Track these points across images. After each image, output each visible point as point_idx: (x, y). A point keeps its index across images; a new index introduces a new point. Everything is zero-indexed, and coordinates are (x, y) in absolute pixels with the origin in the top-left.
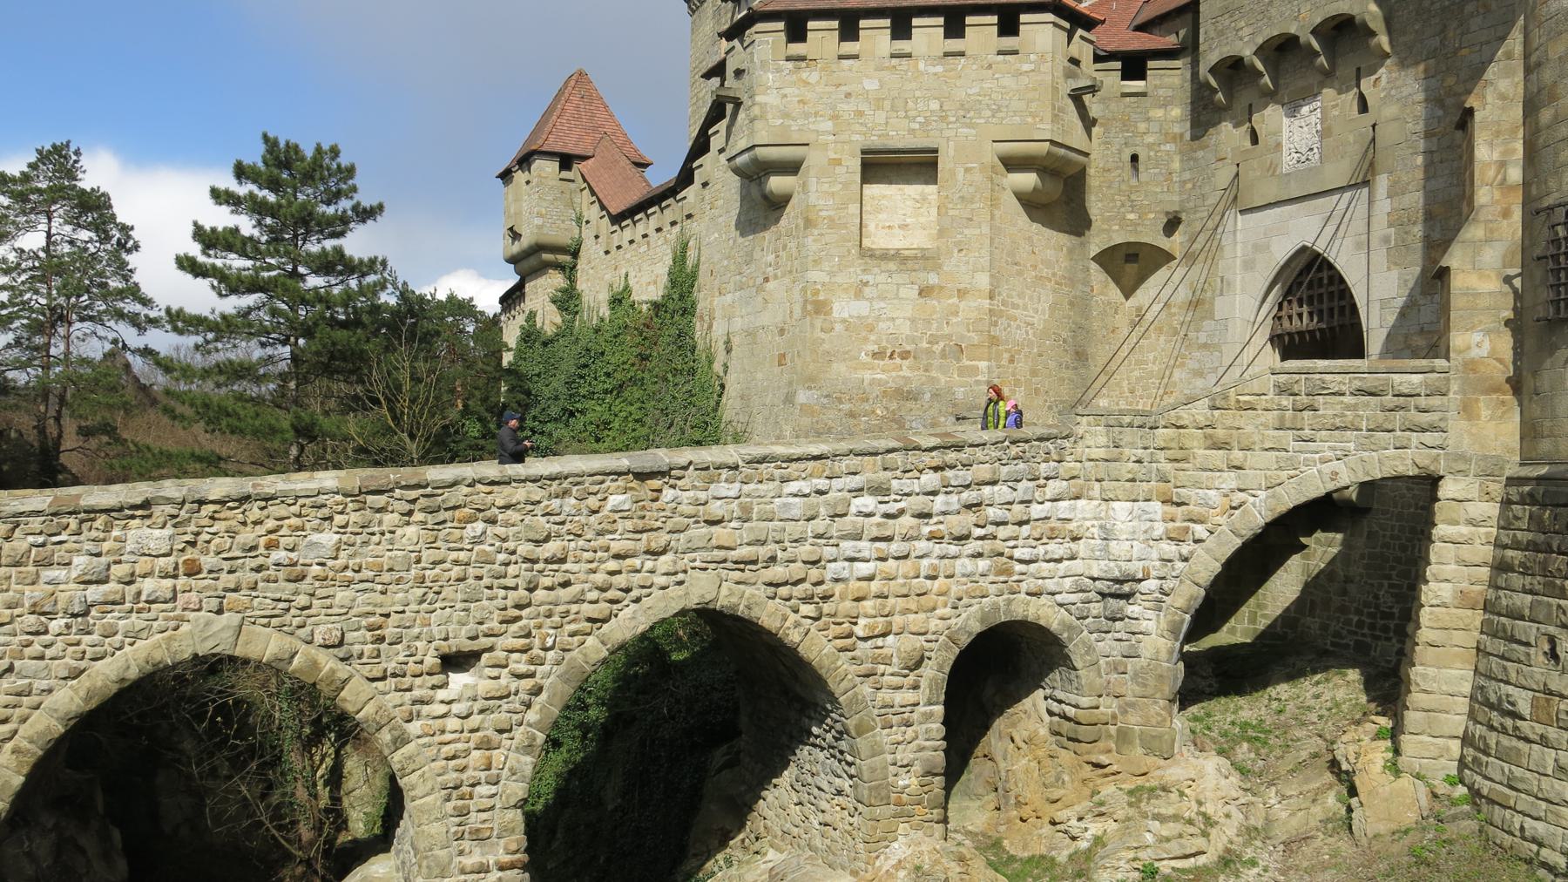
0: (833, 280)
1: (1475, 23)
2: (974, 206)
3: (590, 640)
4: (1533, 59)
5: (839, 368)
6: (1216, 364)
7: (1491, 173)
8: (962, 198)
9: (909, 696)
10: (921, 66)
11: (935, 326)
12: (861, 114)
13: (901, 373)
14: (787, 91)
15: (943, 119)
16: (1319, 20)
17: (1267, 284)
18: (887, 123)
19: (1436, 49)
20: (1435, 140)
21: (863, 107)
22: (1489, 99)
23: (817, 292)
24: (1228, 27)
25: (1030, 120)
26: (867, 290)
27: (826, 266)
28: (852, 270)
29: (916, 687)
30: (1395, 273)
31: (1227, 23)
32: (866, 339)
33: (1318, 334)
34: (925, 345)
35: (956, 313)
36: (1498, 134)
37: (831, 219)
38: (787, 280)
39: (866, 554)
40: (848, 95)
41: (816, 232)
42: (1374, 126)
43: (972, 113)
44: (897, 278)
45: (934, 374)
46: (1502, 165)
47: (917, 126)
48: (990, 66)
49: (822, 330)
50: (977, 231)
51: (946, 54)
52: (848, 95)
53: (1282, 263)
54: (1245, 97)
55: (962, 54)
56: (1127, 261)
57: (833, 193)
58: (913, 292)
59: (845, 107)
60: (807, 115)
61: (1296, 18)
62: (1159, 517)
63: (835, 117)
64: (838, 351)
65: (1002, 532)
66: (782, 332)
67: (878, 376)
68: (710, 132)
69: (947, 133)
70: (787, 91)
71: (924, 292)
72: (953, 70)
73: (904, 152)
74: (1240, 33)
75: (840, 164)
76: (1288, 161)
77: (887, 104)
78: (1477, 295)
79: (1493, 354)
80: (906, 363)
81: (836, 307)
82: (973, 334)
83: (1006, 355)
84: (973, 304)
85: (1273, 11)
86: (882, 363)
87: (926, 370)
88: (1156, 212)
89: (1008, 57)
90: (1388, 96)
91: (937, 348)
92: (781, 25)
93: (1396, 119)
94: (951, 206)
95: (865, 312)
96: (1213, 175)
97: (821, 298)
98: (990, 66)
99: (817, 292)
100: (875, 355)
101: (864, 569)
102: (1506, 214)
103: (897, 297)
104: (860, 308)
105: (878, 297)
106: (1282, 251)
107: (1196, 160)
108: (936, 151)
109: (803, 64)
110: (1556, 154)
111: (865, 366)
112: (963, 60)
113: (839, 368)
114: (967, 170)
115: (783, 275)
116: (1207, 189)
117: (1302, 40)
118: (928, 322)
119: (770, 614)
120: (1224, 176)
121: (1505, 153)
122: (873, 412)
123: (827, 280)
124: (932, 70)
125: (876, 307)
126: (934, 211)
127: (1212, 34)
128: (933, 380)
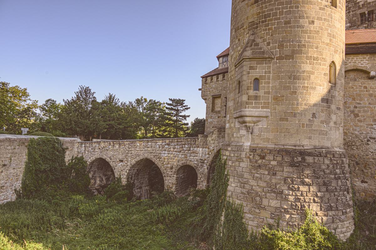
3: (134, 160)
9: (171, 173)
12: (212, 90)
15: (222, 90)
21: (213, 90)
29: (172, 172)
39: (166, 153)
44: (216, 115)
60: (207, 91)
62: (207, 151)
65: (186, 152)
69: (222, 92)
71: (219, 117)
100: (213, 127)
101: (165, 155)
103: (215, 118)
113: (209, 129)
118: (219, 122)
119: (154, 160)
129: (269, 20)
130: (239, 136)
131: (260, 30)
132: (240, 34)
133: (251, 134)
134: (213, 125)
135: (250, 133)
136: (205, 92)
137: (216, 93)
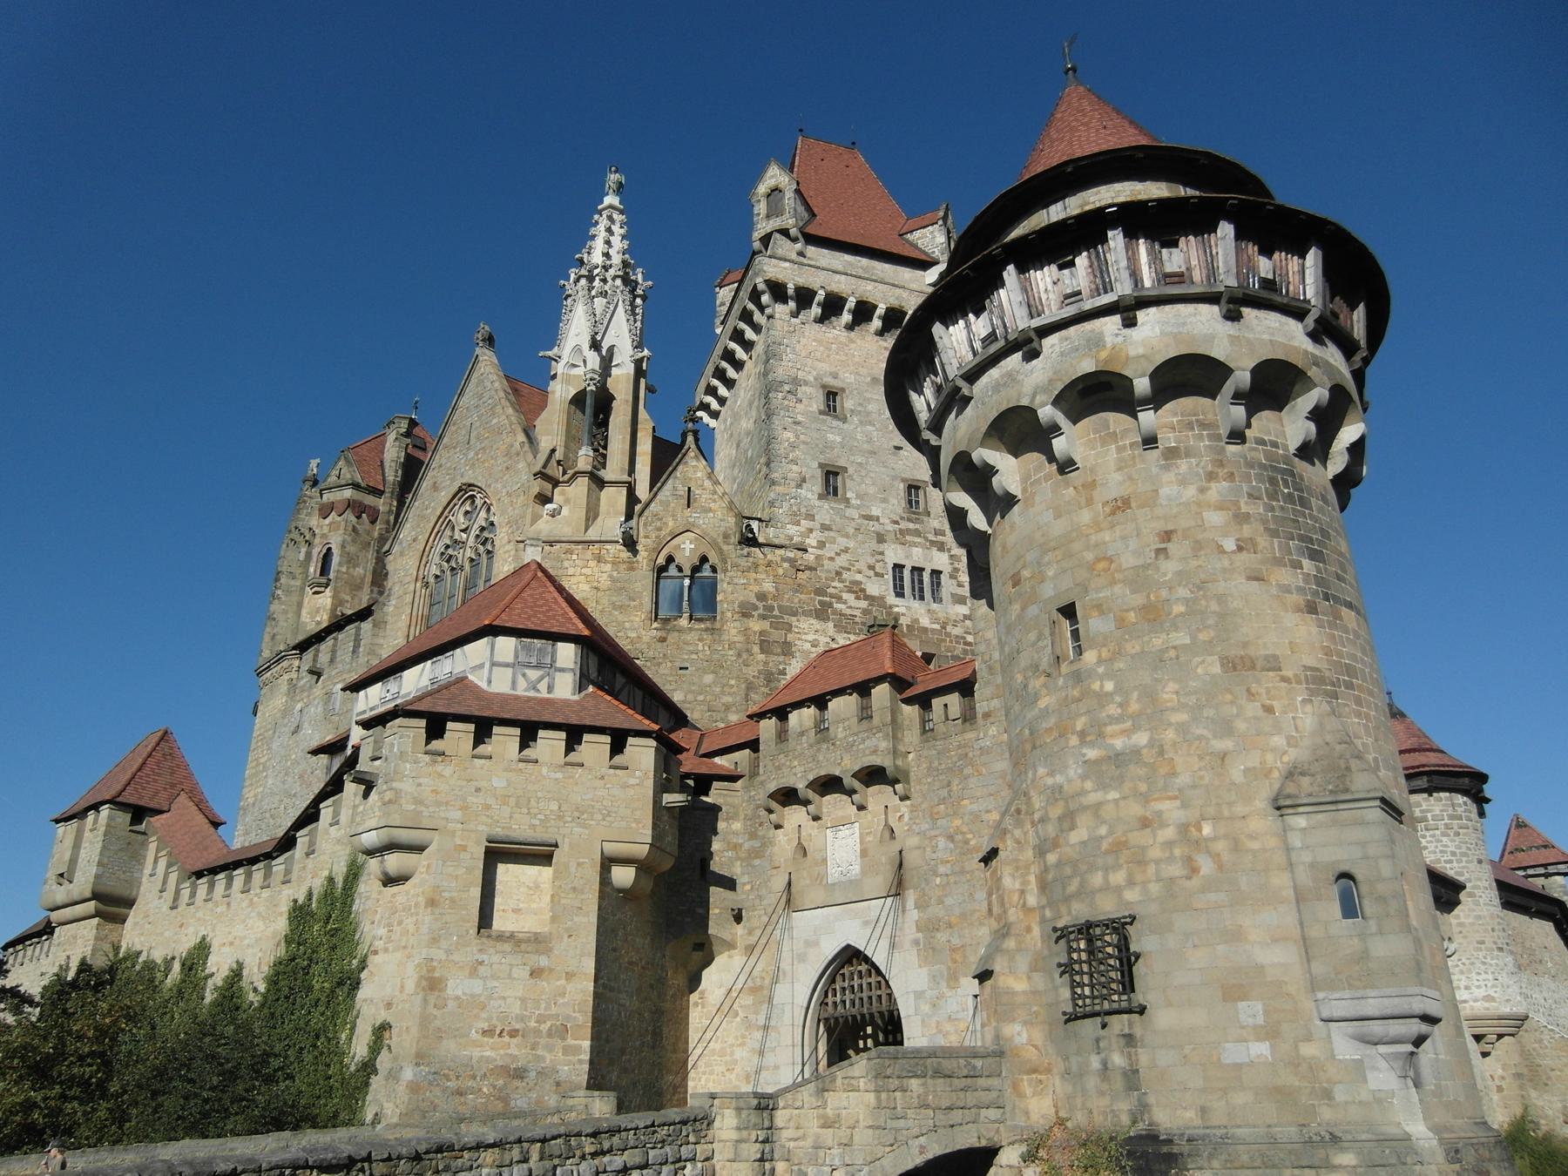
0: (451, 958)
1: (973, 782)
2: (583, 897)
5: (449, 1047)
6: (774, 1044)
7: (1015, 897)
8: (574, 889)
10: (544, 770)
11: (543, 1006)
12: (488, 807)
13: (509, 1051)
14: (421, 780)
15: (560, 818)
16: (857, 768)
17: (817, 975)
18: (511, 817)
19: (944, 798)
20: (949, 865)
21: (491, 801)
22: (1009, 843)
23: (433, 969)
24: (784, 764)
25: (634, 825)
26: (482, 969)
27: (444, 944)
28: (469, 949)
30: (924, 972)
31: (783, 761)
32: (477, 1017)
33: (859, 1017)
34: (533, 1024)
35: (563, 994)
36: (1017, 868)
37: (453, 900)
38: (399, 955)
40: (478, 790)
41: (437, 911)
42: (901, 852)
43: (585, 816)
45: (540, 1052)
46: (1022, 892)
47: (538, 822)
48: (602, 778)
49: (435, 1006)
50: (585, 920)
51: (567, 764)
52: (478, 790)
53: (830, 958)
54: (795, 816)
56: (694, 949)
57: (457, 876)
58: (524, 973)
59: (475, 800)
60: (438, 804)
61: (839, 764)
63: (464, 808)
64: (449, 1028)
66: (389, 1005)
67: (488, 1053)
68: (321, 806)
69: (562, 831)
70: (421, 780)
71: (535, 973)
72: (569, 777)
73: (520, 844)
74: (794, 770)
75: (465, 851)
76: (833, 874)
77: (512, 801)
78: (1014, 993)
79: (1030, 1042)
80: (514, 1041)
81: (450, 983)
82: (577, 1015)
83: (604, 1036)
84: (579, 986)
85: (821, 758)
86: (492, 1040)
87: (533, 1049)
88: (721, 909)
89: (618, 772)
91: (545, 1027)
92: (423, 723)
93: (919, 848)
94: (563, 895)
95: (478, 990)
96: (769, 880)
97: (436, 975)
98: (602, 778)
99: (433, 969)
100: (484, 1033)
102: (1029, 930)
103: (510, 976)
104: (476, 986)
105: (492, 976)
106: (830, 948)
107: (753, 866)
109: (440, 759)
110: (1064, 889)
111: (475, 1044)
112: (580, 770)
114: (579, 864)
115: (396, 949)
116: (763, 892)
117: (845, 782)
120: (779, 883)
121: (1023, 883)
122: (480, 1090)
123: (444, 958)
124: (553, 775)
125: (489, 985)
126: (548, 898)
127: (770, 767)
128: (540, 1059)
129: (1360, 688)
130: (1364, 1095)
131: (1347, 709)
132: (1268, 692)
133: (1416, 1086)
134: (489, 1019)
135: (1410, 1083)
136: (419, 801)
137: (522, 828)
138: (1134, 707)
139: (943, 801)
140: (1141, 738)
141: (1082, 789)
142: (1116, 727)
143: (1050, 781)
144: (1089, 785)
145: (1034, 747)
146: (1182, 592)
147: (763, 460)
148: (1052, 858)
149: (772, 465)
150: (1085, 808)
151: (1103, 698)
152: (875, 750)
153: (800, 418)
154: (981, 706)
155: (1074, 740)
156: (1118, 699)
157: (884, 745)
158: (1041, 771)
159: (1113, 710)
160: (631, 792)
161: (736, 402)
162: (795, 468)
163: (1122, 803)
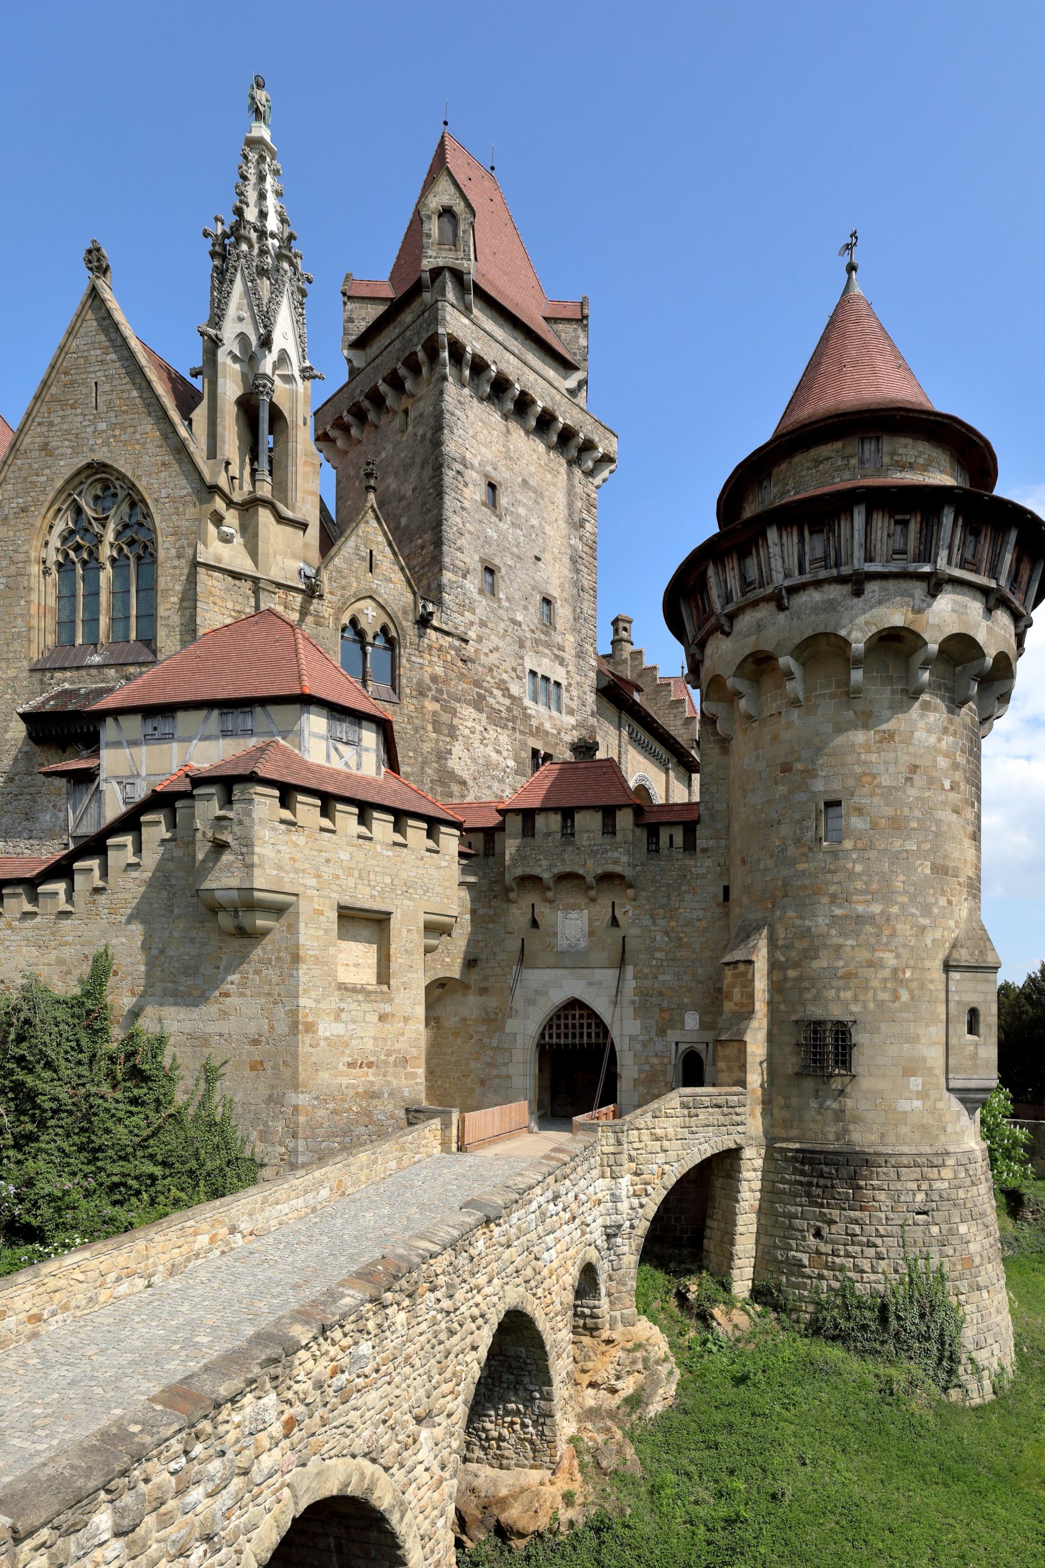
4: (780, 943)
15: (393, 890)
48: (422, 859)
55: (405, 846)
69: (396, 902)
90: (633, 922)
98: (422, 859)
108: (389, 914)
110: (801, 995)
124: (385, 853)
138: (875, 886)
139: (663, 907)
140: (876, 908)
141: (828, 934)
142: (860, 898)
143: (798, 922)
144: (833, 932)
145: (786, 896)
146: (917, 813)
147: (428, 537)
148: (792, 973)
149: (445, 548)
150: (826, 946)
151: (852, 875)
152: (619, 861)
153: (467, 504)
154: (701, 843)
155: (825, 900)
156: (864, 878)
157: (625, 859)
158: (791, 913)
159: (859, 885)
160: (442, 872)
161: (379, 453)
162: (458, 554)
163: (857, 949)
